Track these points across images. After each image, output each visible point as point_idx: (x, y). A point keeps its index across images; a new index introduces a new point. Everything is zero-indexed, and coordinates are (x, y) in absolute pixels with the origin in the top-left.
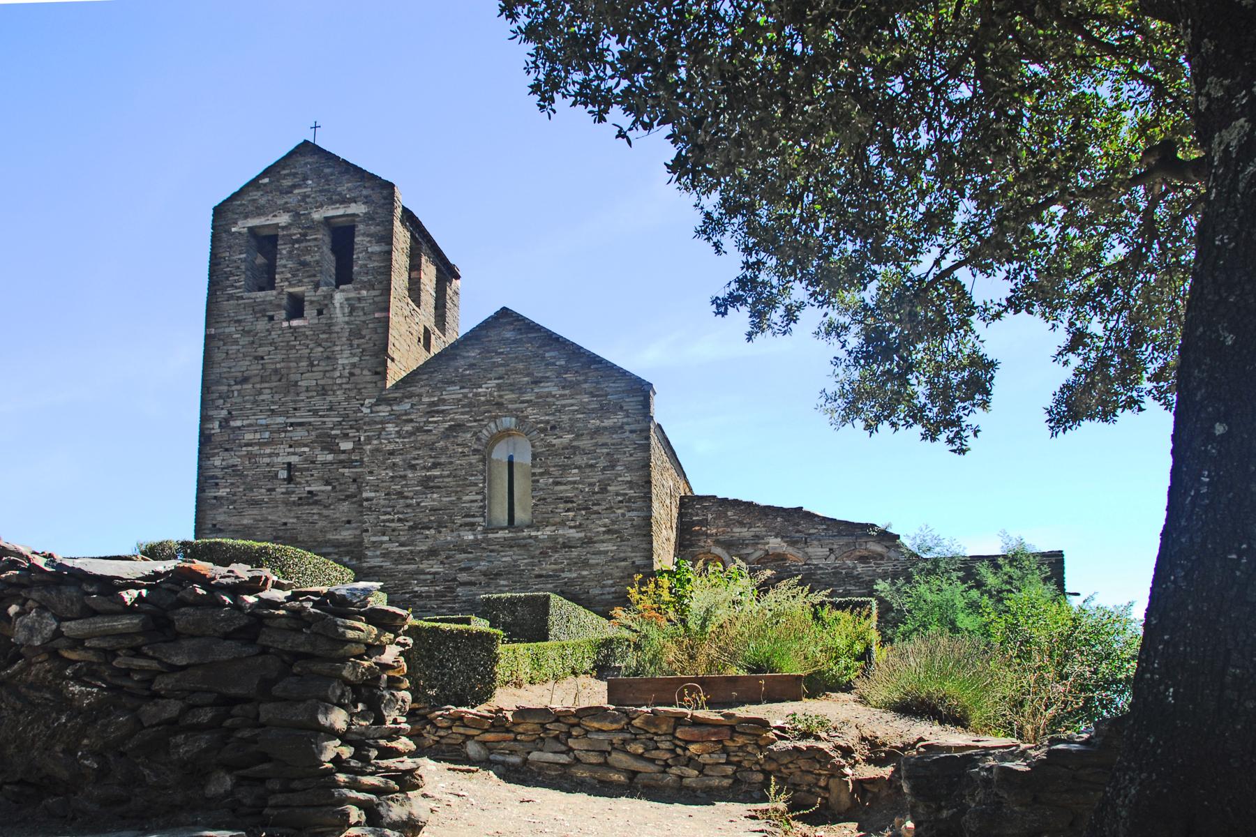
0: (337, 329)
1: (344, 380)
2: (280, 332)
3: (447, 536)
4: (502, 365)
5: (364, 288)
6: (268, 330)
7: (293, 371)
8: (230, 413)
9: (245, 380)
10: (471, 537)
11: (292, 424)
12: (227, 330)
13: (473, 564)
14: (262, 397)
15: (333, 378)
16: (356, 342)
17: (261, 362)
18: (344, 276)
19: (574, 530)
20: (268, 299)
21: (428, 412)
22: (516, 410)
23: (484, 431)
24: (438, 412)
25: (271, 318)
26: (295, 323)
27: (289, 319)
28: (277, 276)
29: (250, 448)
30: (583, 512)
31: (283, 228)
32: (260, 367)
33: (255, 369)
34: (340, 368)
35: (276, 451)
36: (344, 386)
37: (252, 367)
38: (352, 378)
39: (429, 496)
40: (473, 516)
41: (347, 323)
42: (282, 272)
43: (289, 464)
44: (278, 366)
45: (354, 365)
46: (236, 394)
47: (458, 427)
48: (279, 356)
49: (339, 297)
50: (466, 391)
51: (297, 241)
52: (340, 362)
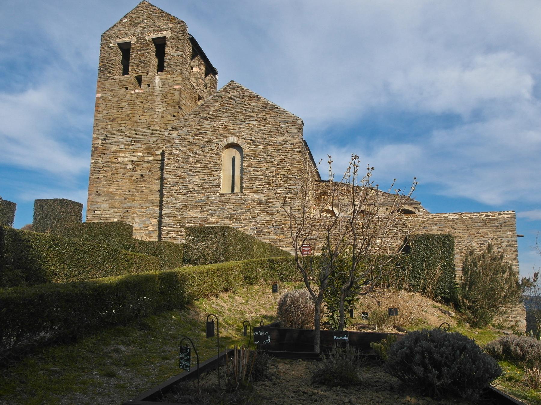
0: (156, 94)
1: (159, 120)
2: (130, 96)
3: (202, 197)
4: (230, 110)
5: (169, 73)
6: (125, 95)
7: (136, 115)
8: (106, 136)
9: (114, 119)
10: (213, 198)
11: (134, 141)
12: (106, 95)
13: (214, 212)
14: (121, 128)
15: (154, 119)
16: (165, 100)
17: (121, 110)
18: (161, 68)
19: (263, 195)
20: (125, 79)
21: (195, 135)
22: (237, 133)
23: (221, 143)
24: (200, 134)
25: (127, 88)
26: (137, 91)
27: (136, 88)
28: (130, 68)
29: (115, 153)
30: (267, 186)
31: (133, 44)
32: (121, 113)
33: (118, 114)
34: (157, 113)
35: (127, 155)
36: (159, 123)
37: (117, 113)
38: (162, 118)
39: (194, 177)
40: (215, 187)
41: (161, 91)
42: (132, 66)
43: (133, 161)
44: (129, 112)
45: (163, 112)
46: (109, 126)
47: (209, 142)
48: (130, 108)
49: (157, 78)
50: (213, 123)
51: (139, 50)
52: (157, 110)
